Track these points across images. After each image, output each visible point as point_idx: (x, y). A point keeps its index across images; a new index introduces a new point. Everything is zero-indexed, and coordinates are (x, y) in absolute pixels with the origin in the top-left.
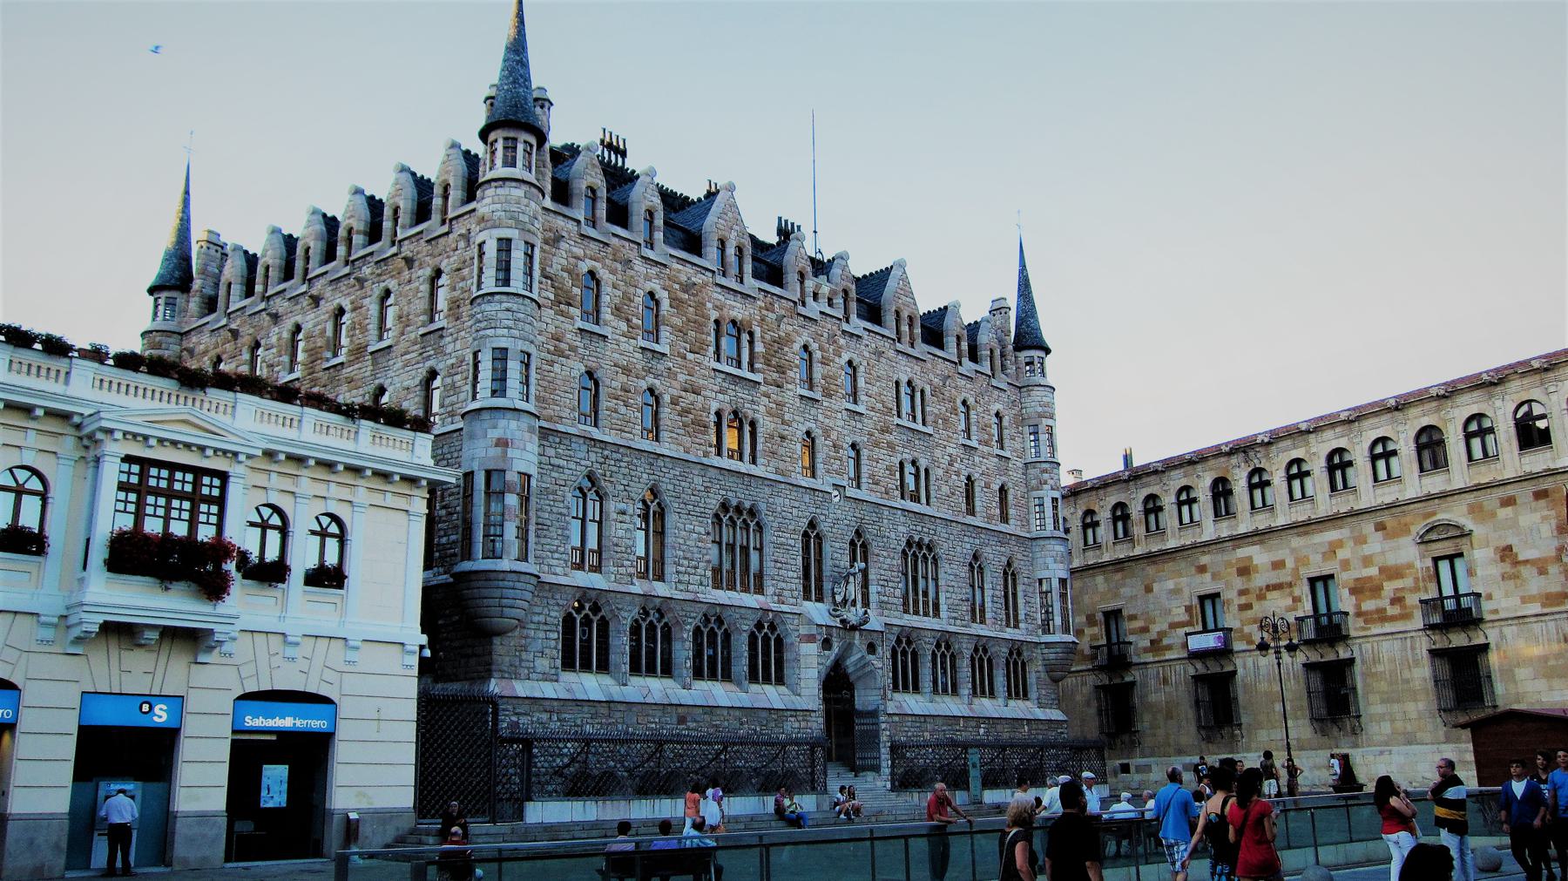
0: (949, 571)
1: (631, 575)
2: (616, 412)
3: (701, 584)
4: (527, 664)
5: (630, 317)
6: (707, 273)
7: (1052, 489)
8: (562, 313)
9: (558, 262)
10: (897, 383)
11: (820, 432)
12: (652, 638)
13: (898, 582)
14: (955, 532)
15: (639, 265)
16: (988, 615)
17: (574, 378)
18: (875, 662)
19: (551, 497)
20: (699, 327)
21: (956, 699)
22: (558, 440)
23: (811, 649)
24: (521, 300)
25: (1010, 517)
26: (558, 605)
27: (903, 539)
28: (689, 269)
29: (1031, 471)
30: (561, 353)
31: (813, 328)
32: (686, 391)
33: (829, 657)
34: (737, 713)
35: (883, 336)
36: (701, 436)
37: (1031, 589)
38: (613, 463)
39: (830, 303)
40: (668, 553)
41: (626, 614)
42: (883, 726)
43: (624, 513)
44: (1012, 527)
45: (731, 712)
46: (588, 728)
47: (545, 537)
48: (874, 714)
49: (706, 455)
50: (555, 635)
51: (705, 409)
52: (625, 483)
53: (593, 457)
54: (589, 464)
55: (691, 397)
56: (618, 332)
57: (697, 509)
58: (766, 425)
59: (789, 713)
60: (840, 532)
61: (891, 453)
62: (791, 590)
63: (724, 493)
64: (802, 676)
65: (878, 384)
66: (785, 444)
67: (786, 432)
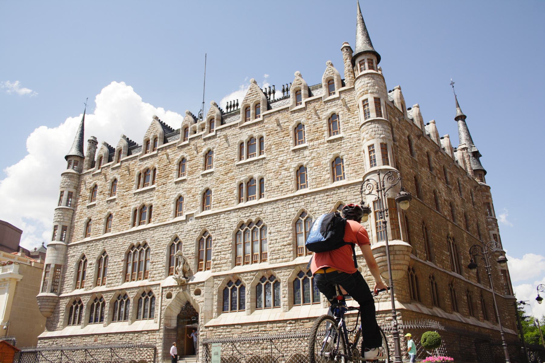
0: (272, 231)
1: (91, 286)
13: (229, 250)
22: (74, 247)
32: (122, 208)
49: (128, 229)
50: (63, 314)
52: (93, 253)
53: (84, 248)
54: (82, 251)
55: (123, 209)
58: (155, 202)
60: (190, 236)
61: (232, 182)
62: (159, 273)
63: (131, 241)
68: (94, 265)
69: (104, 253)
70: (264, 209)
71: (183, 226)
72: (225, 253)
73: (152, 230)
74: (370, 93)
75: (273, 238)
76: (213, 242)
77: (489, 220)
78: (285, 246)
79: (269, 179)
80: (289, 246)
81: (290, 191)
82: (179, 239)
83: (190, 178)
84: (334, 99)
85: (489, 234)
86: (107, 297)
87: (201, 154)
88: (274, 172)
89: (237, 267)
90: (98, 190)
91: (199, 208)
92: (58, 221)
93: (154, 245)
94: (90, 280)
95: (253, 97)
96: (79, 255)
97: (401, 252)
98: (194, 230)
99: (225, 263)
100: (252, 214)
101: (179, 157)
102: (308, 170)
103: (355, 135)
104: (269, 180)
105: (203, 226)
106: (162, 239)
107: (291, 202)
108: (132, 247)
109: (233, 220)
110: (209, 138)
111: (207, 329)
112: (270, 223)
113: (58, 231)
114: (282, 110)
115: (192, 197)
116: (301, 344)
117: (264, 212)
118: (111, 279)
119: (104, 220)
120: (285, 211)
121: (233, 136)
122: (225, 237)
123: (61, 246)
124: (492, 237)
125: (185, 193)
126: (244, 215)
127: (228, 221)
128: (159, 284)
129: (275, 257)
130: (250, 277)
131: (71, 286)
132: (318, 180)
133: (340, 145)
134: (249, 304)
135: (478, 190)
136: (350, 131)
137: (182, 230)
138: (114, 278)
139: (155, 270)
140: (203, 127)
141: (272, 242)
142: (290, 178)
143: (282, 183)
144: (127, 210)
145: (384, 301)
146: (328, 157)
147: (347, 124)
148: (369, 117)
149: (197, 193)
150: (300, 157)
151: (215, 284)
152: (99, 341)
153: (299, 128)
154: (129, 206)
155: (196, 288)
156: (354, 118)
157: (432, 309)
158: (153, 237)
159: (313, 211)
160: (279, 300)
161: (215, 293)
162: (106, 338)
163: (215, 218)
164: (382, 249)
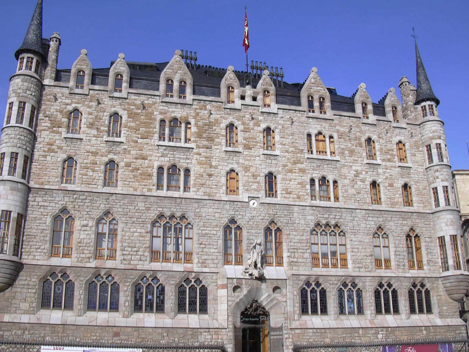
0: (354, 239)
1: (89, 258)
2: (87, 175)
3: (140, 260)
4: (16, 306)
5: (99, 127)
6: (156, 97)
7: (442, 181)
8: (54, 132)
10: (309, 135)
11: (241, 169)
13: (307, 249)
14: (359, 216)
15: (107, 101)
16: (393, 263)
17: (59, 162)
18: (280, 298)
19: (37, 222)
21: (361, 317)
22: (44, 193)
23: (222, 293)
24: (13, 129)
25: (414, 202)
27: (312, 223)
28: (143, 98)
29: (429, 172)
30: (50, 150)
31: (237, 114)
32: (136, 159)
33: (238, 297)
34: (160, 330)
35: (296, 110)
36: (145, 181)
37: (433, 244)
38: (80, 201)
39: (254, 99)
40: (119, 245)
41: (82, 279)
42: (286, 336)
43: (86, 226)
44: (416, 207)
45: (155, 329)
47: (33, 241)
48: (280, 329)
49: (150, 190)
50: (34, 291)
52: (86, 210)
53: (67, 199)
54: (65, 203)
55: (140, 161)
56: (91, 135)
58: (195, 169)
59: (202, 330)
63: (161, 209)
64: (219, 309)
65: (291, 137)
66: (211, 179)
67: (213, 172)
68: (94, 229)
70: (344, 215)
71: (245, 209)
72: (303, 251)
73: (196, 202)
75: (355, 247)
79: (345, 184)
80: (371, 258)
81: (366, 203)
83: (248, 153)
86: (126, 277)
89: (315, 269)
90: (84, 120)
91: (263, 192)
93: (201, 224)
94: (86, 248)
95: (318, 88)
96: (54, 208)
98: (260, 217)
99: (304, 262)
100: (331, 216)
102: (382, 188)
103: (422, 170)
104: (345, 186)
106: (213, 218)
108: (161, 216)
109: (308, 217)
111: (293, 332)
115: (252, 177)
117: (344, 218)
118: (129, 254)
119: (103, 167)
122: (301, 234)
126: (322, 216)
128: (218, 273)
129: (358, 265)
130: (335, 282)
131: (45, 251)
132: (392, 201)
134: (335, 309)
136: (417, 164)
138: (135, 253)
139: (206, 255)
140: (255, 96)
141: (354, 250)
142: (366, 190)
143: (358, 193)
144: (147, 165)
145: (451, 318)
146: (400, 182)
147: (414, 157)
148: (442, 161)
149: (259, 174)
150: (374, 173)
151: (295, 283)
152: (123, 337)
154: (150, 160)
159: (391, 229)
161: (295, 293)
162: (136, 333)
163: (286, 210)
164: (461, 276)
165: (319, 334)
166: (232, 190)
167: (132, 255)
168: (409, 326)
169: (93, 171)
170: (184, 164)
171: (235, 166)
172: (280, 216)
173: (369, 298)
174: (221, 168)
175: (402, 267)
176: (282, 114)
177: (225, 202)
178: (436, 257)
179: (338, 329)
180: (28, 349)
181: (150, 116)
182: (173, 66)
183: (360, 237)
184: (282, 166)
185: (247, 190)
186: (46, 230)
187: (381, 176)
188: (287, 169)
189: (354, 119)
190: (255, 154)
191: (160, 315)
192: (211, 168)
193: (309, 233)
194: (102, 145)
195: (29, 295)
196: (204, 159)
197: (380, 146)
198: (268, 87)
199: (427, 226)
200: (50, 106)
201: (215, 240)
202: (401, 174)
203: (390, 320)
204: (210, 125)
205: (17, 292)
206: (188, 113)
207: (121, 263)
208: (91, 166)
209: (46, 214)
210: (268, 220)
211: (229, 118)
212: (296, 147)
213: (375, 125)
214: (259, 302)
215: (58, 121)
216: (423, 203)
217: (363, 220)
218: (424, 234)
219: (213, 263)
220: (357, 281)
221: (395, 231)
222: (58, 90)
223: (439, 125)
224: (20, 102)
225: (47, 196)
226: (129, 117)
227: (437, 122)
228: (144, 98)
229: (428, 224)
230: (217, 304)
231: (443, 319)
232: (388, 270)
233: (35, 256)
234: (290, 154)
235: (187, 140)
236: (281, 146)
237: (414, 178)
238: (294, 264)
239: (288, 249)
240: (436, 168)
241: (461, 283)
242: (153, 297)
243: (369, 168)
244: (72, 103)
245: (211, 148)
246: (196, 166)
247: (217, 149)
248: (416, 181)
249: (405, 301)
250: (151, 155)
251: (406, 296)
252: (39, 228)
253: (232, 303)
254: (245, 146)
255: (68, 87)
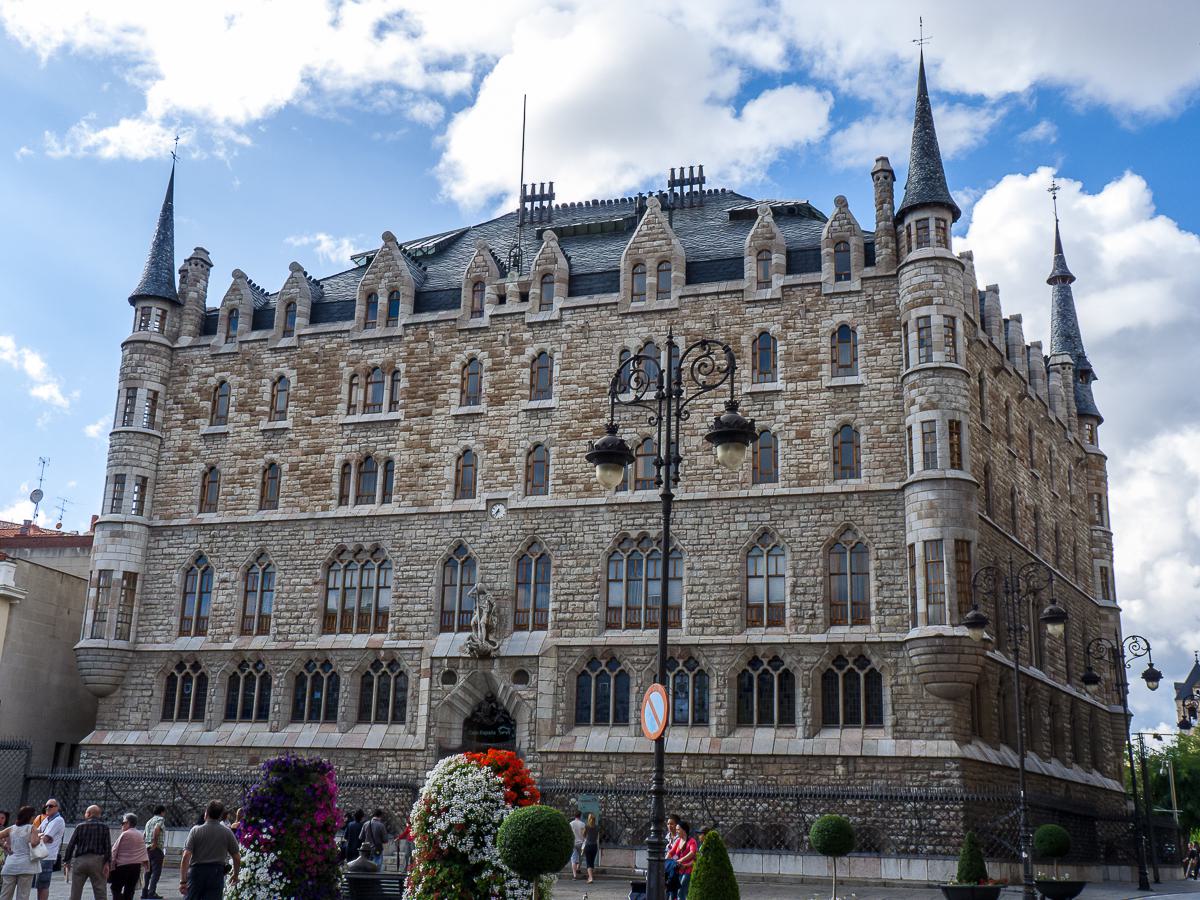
0: (697, 566)
1: (228, 634)
3: (303, 632)
6: (343, 335)
7: (922, 409)
8: (189, 428)
9: (188, 391)
11: (481, 446)
12: (249, 686)
13: (593, 594)
14: (715, 513)
15: (268, 358)
17: (195, 477)
18: (523, 693)
19: (161, 581)
20: (329, 389)
21: (698, 732)
22: (170, 533)
23: (425, 683)
26: (154, 668)
27: (608, 540)
30: (184, 460)
32: (307, 454)
35: (598, 306)
37: (896, 564)
38: (220, 539)
42: (530, 766)
46: (160, 769)
47: (153, 614)
49: (325, 508)
51: (331, 466)
52: (229, 554)
53: (201, 539)
55: (312, 458)
57: (306, 562)
58: (402, 457)
62: (417, 624)
63: (339, 540)
65: (583, 365)
66: (429, 473)
69: (261, 554)
71: (479, 524)
72: (585, 597)
74: (936, 304)
76: (553, 571)
77: (1095, 534)
78: (725, 600)
80: (732, 603)
82: (466, 551)
84: (849, 293)
85: (1092, 568)
86: (278, 664)
87: (525, 358)
88: (702, 435)
89: (609, 633)
90: (233, 399)
91: (519, 487)
92: (125, 465)
95: (655, 243)
96: (184, 554)
97: (973, 651)
98: (507, 538)
99: (584, 620)
100: (650, 521)
101: (462, 357)
103: (890, 386)
104: (690, 451)
105: (530, 532)
107: (740, 510)
108: (341, 551)
109: (602, 528)
110: (543, 324)
111: (544, 759)
112: (691, 547)
113: (131, 489)
114: (726, 293)
115: (500, 460)
116: (754, 805)
117: (678, 521)
118: (287, 624)
119: (258, 478)
120: (726, 526)
121: (605, 332)
123: (136, 528)
124: (1098, 574)
125: (481, 446)
126: (631, 522)
127: (592, 528)
128: (421, 648)
131: (168, 627)
132: (801, 470)
133: (856, 402)
135: (1082, 467)
137: (477, 533)
140: (524, 290)
141: (695, 589)
145: (927, 739)
148: (929, 358)
150: (764, 413)
153: (764, 344)
154: (329, 453)
155: (517, 669)
156: (889, 347)
157: (998, 750)
158: (402, 538)
160: (707, 711)
161: (560, 683)
163: (559, 517)
164: (937, 641)
165: (594, 765)
166: (464, 487)
167: (290, 624)
168: (800, 753)
169: (243, 485)
170: (382, 453)
171: (470, 442)
172: (544, 531)
173: (715, 692)
174: (445, 450)
175: (808, 621)
176: (571, 319)
177: (445, 516)
178: (902, 593)
179: (635, 756)
180: (134, 786)
181: (333, 374)
182: (376, 267)
183: (710, 560)
184: (561, 428)
185: (490, 486)
186: (171, 593)
187: (778, 417)
188: (570, 432)
189: (728, 296)
190: (509, 412)
191: (328, 727)
192: (426, 452)
193: (603, 558)
194: (257, 438)
195: (142, 699)
196: (417, 437)
197: (785, 348)
198: (549, 266)
199: (886, 521)
200: (184, 385)
201: (424, 588)
202: (831, 405)
203: (763, 740)
204: (432, 369)
205: (127, 696)
206: (394, 355)
207: (274, 640)
208: (240, 477)
209: (171, 567)
210: (521, 540)
211: (468, 348)
212: (590, 384)
213: (779, 299)
214: (498, 700)
215: (196, 407)
216: (886, 468)
217: (721, 521)
218: (874, 540)
219: (419, 631)
220: (695, 653)
221: (798, 539)
222: (195, 352)
223: (931, 270)
224: (128, 389)
225: (174, 537)
226: (299, 382)
227: (925, 263)
228: (324, 340)
229: (891, 517)
230: (417, 705)
231: (903, 741)
232: (775, 629)
233: (154, 637)
234: (579, 401)
235: (393, 405)
236: (561, 388)
237: (867, 410)
238: (565, 624)
239: (556, 595)
240: (913, 378)
241: (939, 656)
242: (321, 695)
243: (751, 402)
244: (215, 372)
245: (430, 414)
246: (403, 453)
247: (443, 414)
248: (870, 415)
249: (805, 697)
250: (330, 445)
251: (806, 687)
252: (162, 590)
253: (436, 703)
254: (491, 401)
255: (209, 345)
